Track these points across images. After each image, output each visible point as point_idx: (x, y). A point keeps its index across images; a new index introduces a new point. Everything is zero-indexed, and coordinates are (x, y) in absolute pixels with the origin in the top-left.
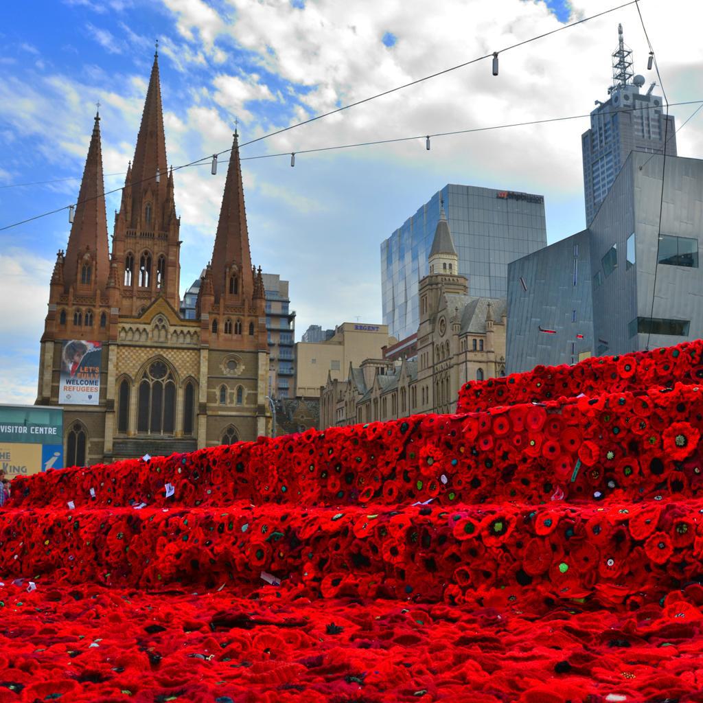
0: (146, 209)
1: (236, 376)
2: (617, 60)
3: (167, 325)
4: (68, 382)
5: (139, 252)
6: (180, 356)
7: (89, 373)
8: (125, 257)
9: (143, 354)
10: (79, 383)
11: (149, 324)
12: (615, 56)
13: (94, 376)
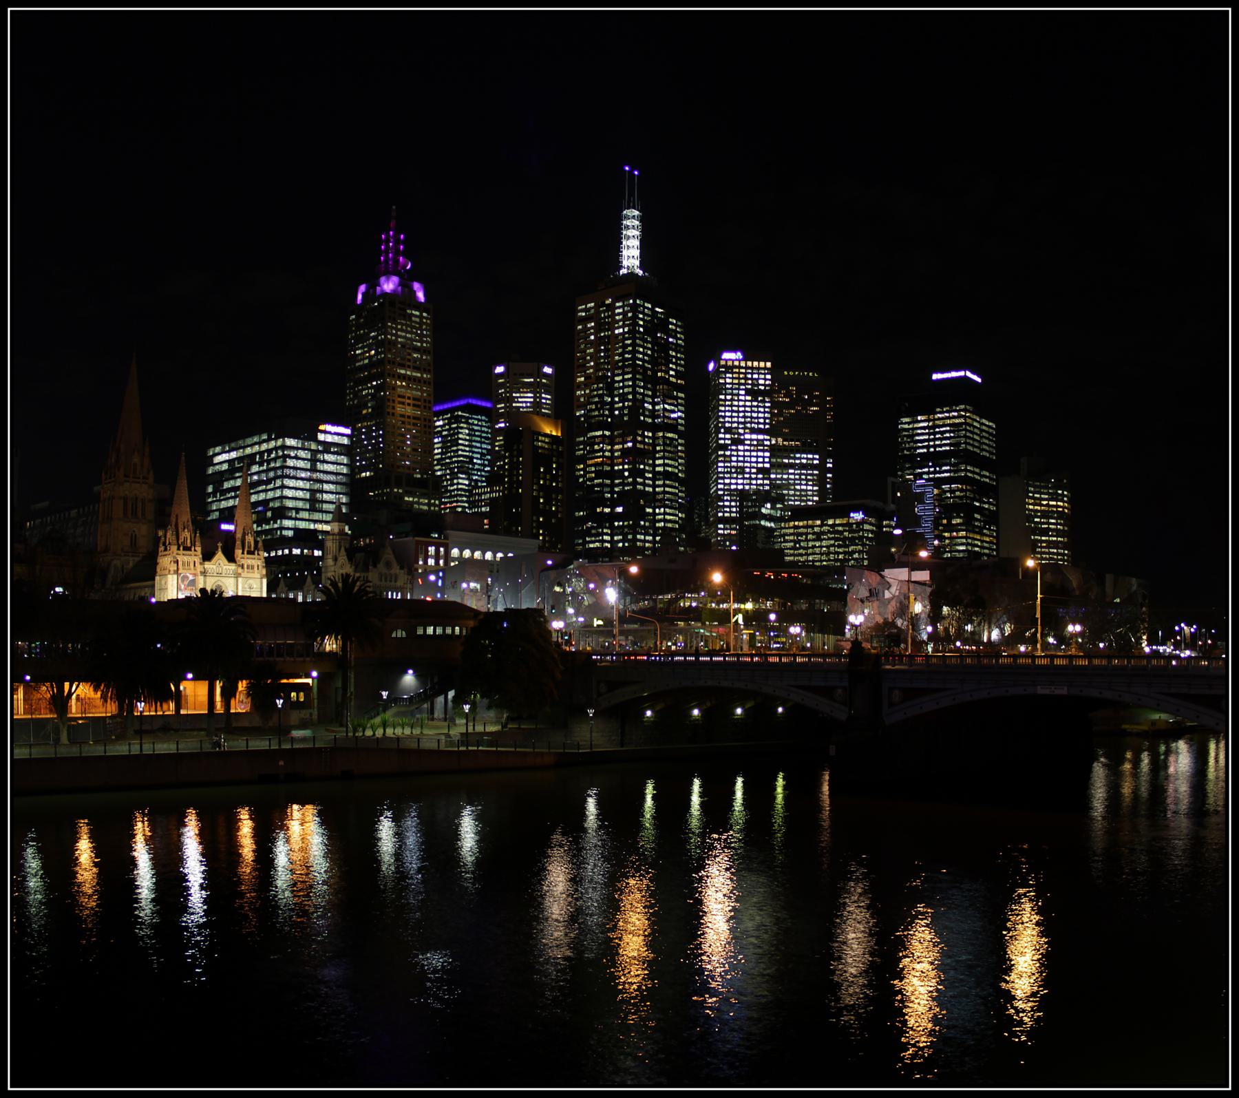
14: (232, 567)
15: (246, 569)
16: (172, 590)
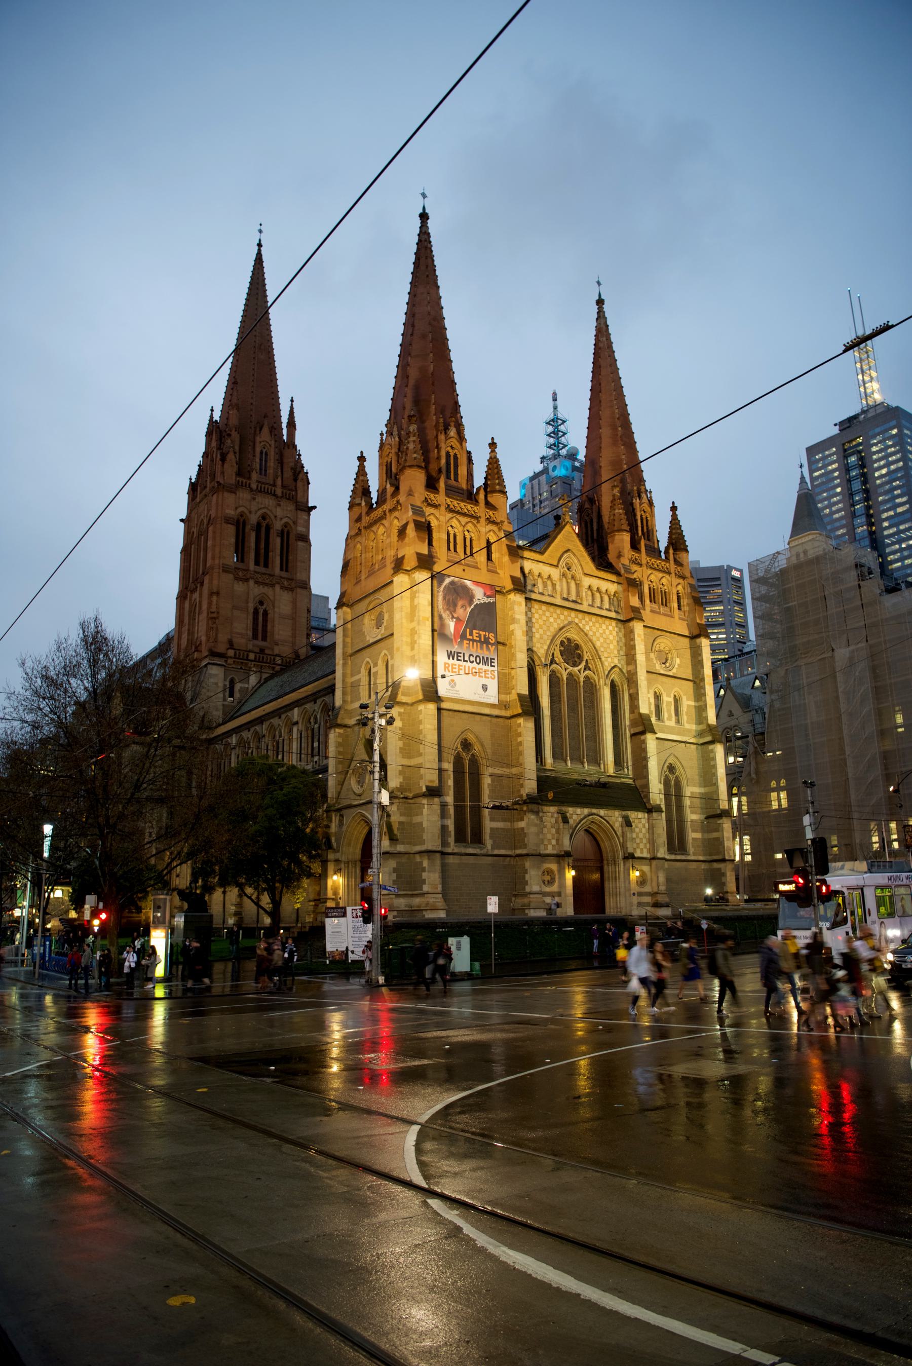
0: (261, 453)
1: (670, 673)
2: (550, 429)
3: (579, 574)
4: (450, 655)
5: (256, 512)
6: (601, 631)
7: (480, 641)
8: (236, 518)
9: (551, 620)
10: (467, 658)
11: (557, 566)
12: (548, 423)
13: (488, 649)
14: (609, 585)
15: (647, 601)
16: (413, 632)
